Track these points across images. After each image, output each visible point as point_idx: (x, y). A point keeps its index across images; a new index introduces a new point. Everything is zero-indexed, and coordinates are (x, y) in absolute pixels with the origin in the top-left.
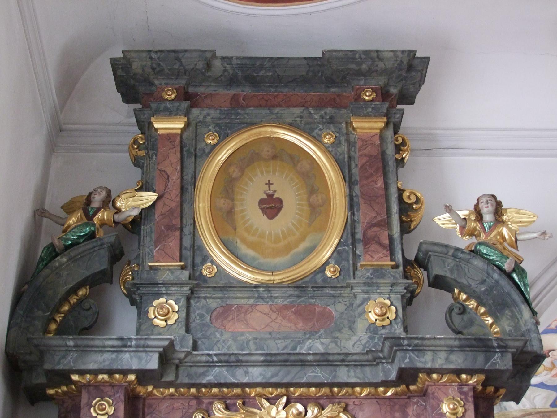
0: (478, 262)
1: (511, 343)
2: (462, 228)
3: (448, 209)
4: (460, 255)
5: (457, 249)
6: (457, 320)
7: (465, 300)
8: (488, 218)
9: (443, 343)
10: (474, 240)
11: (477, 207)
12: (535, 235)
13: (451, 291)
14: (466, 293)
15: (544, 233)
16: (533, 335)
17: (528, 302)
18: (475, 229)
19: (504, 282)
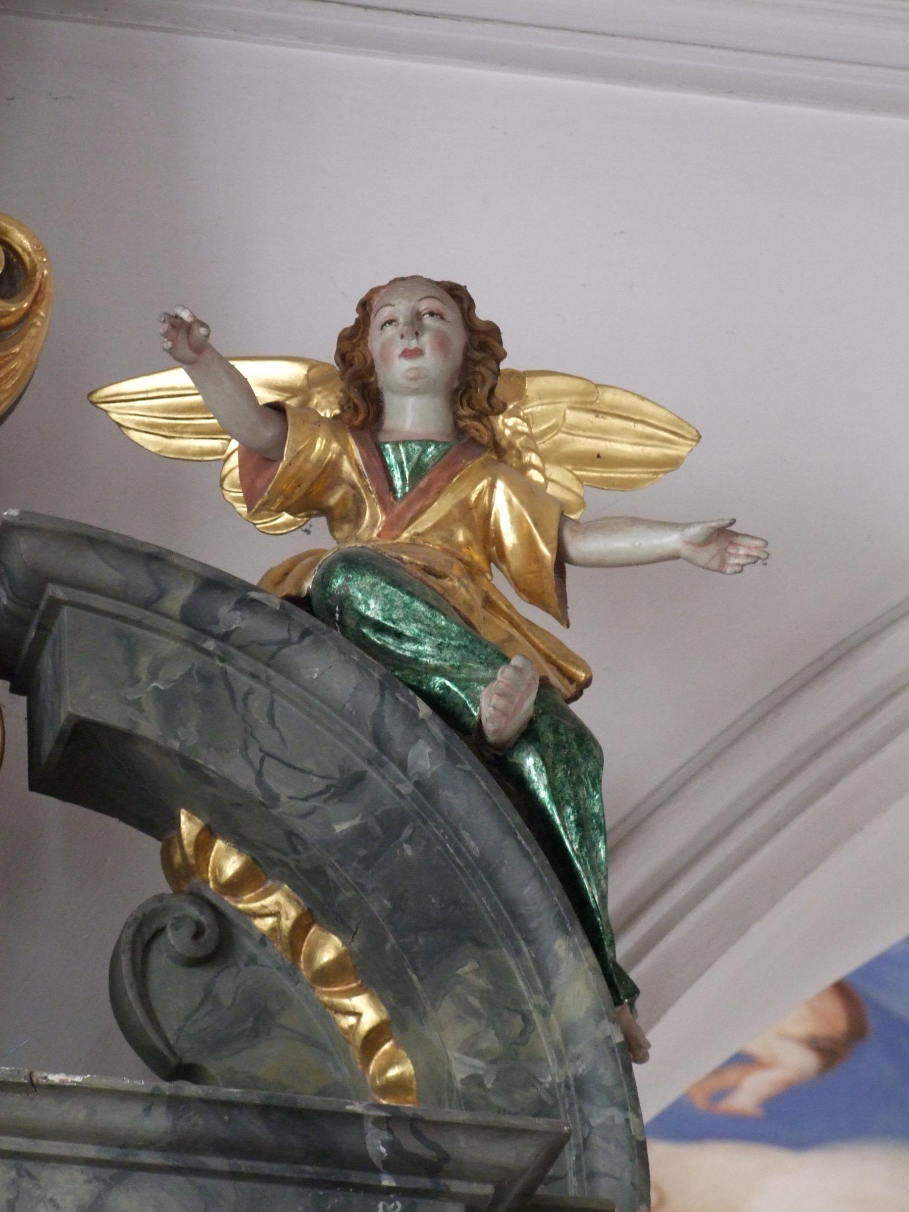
0: (328, 670)
1: (468, 1149)
2: (259, 460)
3: (188, 343)
4: (228, 616)
5: (216, 583)
6: (177, 994)
7: (236, 886)
8: (413, 414)
9: (75, 1114)
10: (320, 538)
11: (353, 340)
12: (671, 540)
13: (162, 827)
14: (240, 842)
15: (723, 534)
16: (603, 1115)
17: (589, 924)
18: (329, 473)
19: (469, 800)
